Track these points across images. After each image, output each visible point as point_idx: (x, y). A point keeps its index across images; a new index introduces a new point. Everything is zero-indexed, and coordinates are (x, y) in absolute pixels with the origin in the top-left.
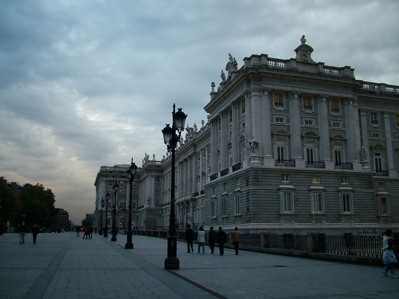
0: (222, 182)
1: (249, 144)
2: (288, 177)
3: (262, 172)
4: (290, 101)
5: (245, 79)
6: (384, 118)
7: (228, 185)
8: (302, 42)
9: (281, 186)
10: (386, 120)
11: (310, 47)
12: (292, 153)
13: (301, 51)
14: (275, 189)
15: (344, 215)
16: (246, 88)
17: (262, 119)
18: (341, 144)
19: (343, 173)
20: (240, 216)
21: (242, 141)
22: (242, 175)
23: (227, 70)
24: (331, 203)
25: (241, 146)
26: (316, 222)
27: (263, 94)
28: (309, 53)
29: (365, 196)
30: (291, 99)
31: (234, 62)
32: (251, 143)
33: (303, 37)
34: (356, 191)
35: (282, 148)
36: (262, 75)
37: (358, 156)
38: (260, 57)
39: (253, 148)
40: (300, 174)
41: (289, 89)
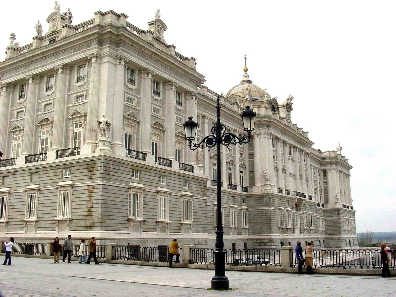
0: (27, 172)
1: (97, 124)
2: (138, 174)
3: (114, 163)
4: (142, 80)
5: (96, 38)
6: (204, 122)
7: (42, 176)
8: (157, 16)
9: (131, 184)
10: (206, 124)
11: (165, 25)
12: (140, 144)
13: (156, 26)
14: (125, 187)
15: (185, 224)
16: (96, 49)
17: (114, 95)
18: (181, 142)
19: (185, 176)
20: (71, 220)
21: (73, 118)
22: (78, 164)
23: (48, 22)
24: (175, 209)
25: (70, 124)
26: (161, 232)
27: (120, 63)
28: (162, 30)
29: (201, 203)
30: (144, 79)
31: (68, 14)
32: (101, 122)
33: (159, 11)
34: (196, 198)
35: (130, 136)
36: (122, 38)
37: (196, 158)
38: (118, 16)
39: (104, 130)
40: (149, 171)
41: (145, 65)
